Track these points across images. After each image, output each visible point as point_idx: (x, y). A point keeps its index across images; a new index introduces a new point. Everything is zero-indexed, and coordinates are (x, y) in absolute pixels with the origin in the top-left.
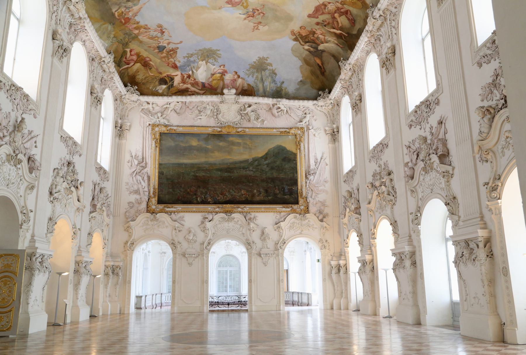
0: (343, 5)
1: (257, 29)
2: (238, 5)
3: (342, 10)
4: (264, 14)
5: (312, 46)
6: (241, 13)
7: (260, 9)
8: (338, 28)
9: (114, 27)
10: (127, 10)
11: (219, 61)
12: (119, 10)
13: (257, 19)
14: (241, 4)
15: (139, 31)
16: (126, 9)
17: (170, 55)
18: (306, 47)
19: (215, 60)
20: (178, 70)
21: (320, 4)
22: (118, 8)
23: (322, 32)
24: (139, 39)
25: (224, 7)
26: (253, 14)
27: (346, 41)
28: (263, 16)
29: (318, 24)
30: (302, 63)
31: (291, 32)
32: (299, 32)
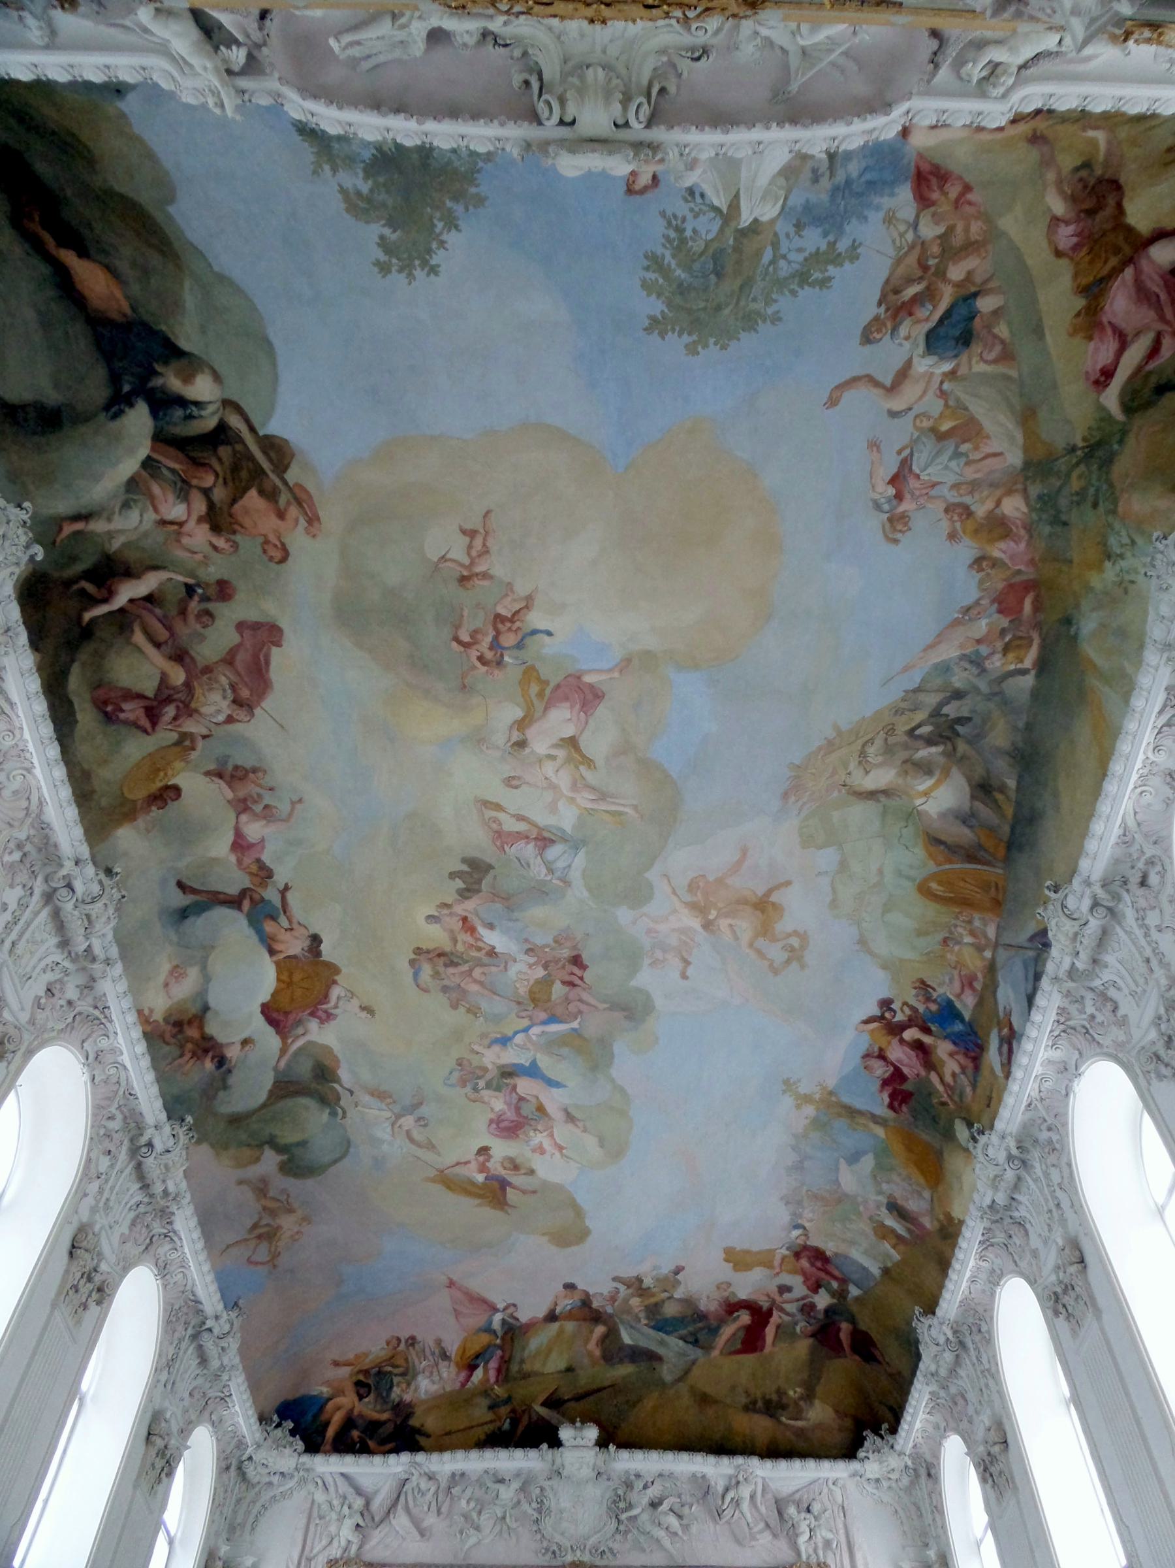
0: (184, 736)
1: (471, 534)
2: (558, 686)
3: (170, 711)
4: (456, 639)
5: (179, 413)
6: (546, 638)
7: (474, 668)
8: (139, 616)
9: (1077, 606)
10: (984, 650)
11: (658, 227)
12: (1012, 667)
13: (478, 605)
14: (548, 691)
15: (998, 503)
16: (987, 658)
17: (925, 268)
18: (202, 389)
19: (680, 230)
20: (920, 155)
21: (258, 704)
22: (1011, 681)
23: (185, 540)
24: (1026, 450)
25: (610, 670)
26: (498, 633)
27: (68, 583)
28: (457, 627)
29: (224, 590)
30: (170, 218)
31: (318, 519)
32: (281, 515)
